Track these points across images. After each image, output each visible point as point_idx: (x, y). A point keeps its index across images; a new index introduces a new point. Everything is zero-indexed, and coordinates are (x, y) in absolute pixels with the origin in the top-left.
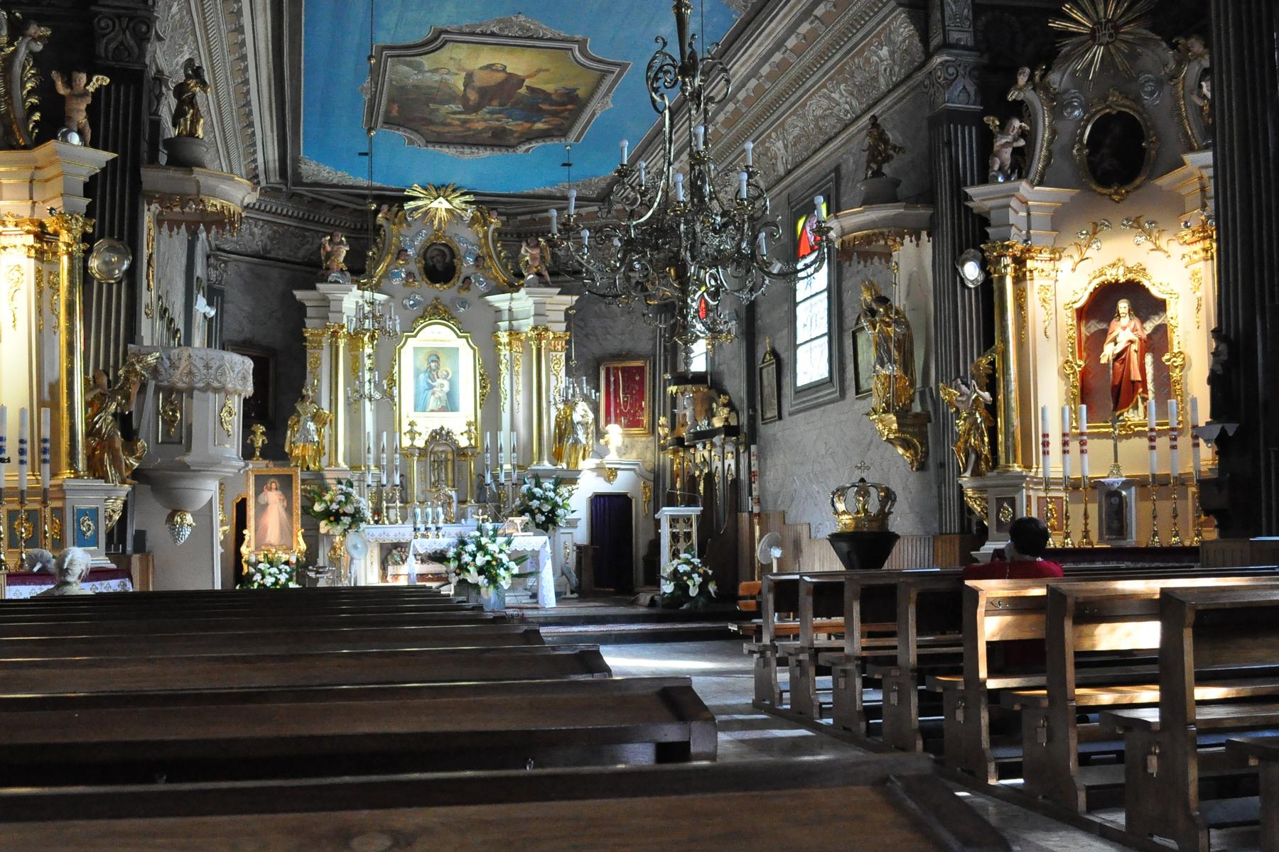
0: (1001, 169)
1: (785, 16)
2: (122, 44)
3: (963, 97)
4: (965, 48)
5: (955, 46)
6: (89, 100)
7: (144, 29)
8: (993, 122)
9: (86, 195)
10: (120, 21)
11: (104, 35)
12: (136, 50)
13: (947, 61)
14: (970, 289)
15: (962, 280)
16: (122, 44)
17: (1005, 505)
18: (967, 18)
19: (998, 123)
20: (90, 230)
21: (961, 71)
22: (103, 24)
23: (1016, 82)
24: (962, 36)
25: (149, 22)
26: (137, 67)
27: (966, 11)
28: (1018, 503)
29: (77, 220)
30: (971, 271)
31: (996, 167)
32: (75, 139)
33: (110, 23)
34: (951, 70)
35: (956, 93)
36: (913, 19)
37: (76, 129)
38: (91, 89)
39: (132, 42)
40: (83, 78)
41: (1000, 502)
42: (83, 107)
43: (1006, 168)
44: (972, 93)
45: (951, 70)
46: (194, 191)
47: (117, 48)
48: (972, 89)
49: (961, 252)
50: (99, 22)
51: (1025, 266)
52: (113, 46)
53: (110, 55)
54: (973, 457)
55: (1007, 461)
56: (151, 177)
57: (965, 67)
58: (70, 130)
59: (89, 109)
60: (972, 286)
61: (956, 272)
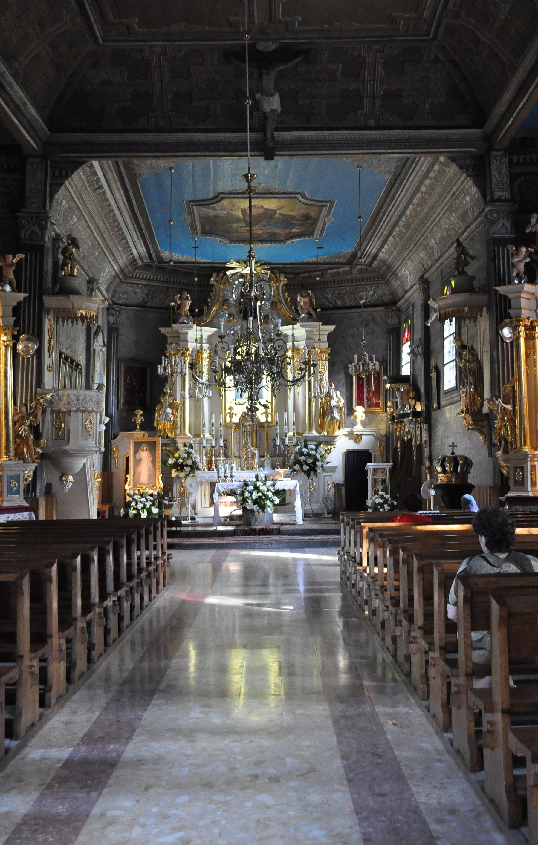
0: (518, 275)
1: (48, 430)
2: (33, 231)
3: (503, 230)
4: (505, 201)
5: (499, 200)
6: (14, 268)
7: (44, 223)
8: (512, 248)
9: (13, 316)
10: (32, 220)
11: (24, 228)
12: (40, 234)
13: (492, 210)
14: (507, 343)
15: (502, 338)
16: (33, 231)
17: (518, 471)
18: (506, 183)
19: (515, 249)
20: (16, 333)
21: (501, 214)
22: (23, 222)
23: (530, 222)
24: (505, 194)
25: (47, 218)
26: (42, 243)
27: (505, 178)
28: (525, 469)
29: (9, 329)
30: (506, 332)
31: (515, 274)
32: (8, 288)
33: (27, 221)
34: (495, 215)
35: (498, 228)
36: (476, 183)
37: (8, 282)
38: (15, 261)
39: (38, 230)
40: (11, 256)
41: (516, 468)
42: (12, 270)
43: (521, 274)
44: (509, 228)
45: (495, 215)
46: (71, 307)
47: (30, 234)
48: (508, 226)
49: (501, 321)
50: (21, 221)
51: (535, 330)
52: (28, 233)
53: (27, 237)
54: (503, 443)
55: (521, 445)
56: (49, 301)
57: (504, 212)
58: (5, 284)
59: (14, 271)
60: (508, 341)
61: (498, 333)
